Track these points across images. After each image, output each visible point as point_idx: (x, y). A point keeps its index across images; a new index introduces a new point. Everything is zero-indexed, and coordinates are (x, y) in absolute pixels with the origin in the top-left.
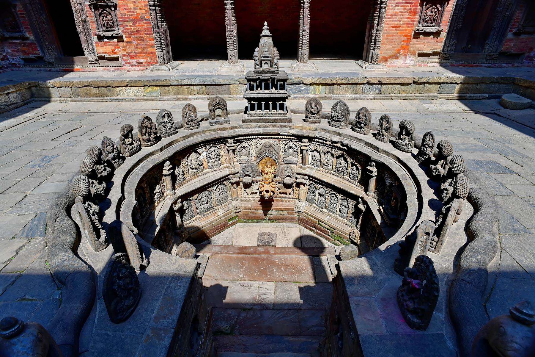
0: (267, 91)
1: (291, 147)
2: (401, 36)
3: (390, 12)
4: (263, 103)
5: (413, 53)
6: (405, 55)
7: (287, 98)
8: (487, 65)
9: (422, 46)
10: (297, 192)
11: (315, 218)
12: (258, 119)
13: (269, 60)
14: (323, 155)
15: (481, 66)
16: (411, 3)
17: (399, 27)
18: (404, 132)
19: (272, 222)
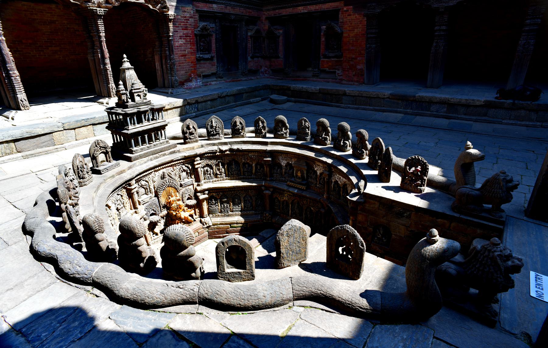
0: (140, 125)
1: (184, 171)
2: (189, 62)
3: (177, 44)
4: (146, 136)
5: (200, 76)
6: (195, 78)
7: (166, 125)
8: (244, 79)
9: (204, 69)
12: (147, 153)
13: (140, 92)
14: (214, 167)
15: (242, 80)
16: (189, 36)
17: (186, 55)
18: (280, 125)
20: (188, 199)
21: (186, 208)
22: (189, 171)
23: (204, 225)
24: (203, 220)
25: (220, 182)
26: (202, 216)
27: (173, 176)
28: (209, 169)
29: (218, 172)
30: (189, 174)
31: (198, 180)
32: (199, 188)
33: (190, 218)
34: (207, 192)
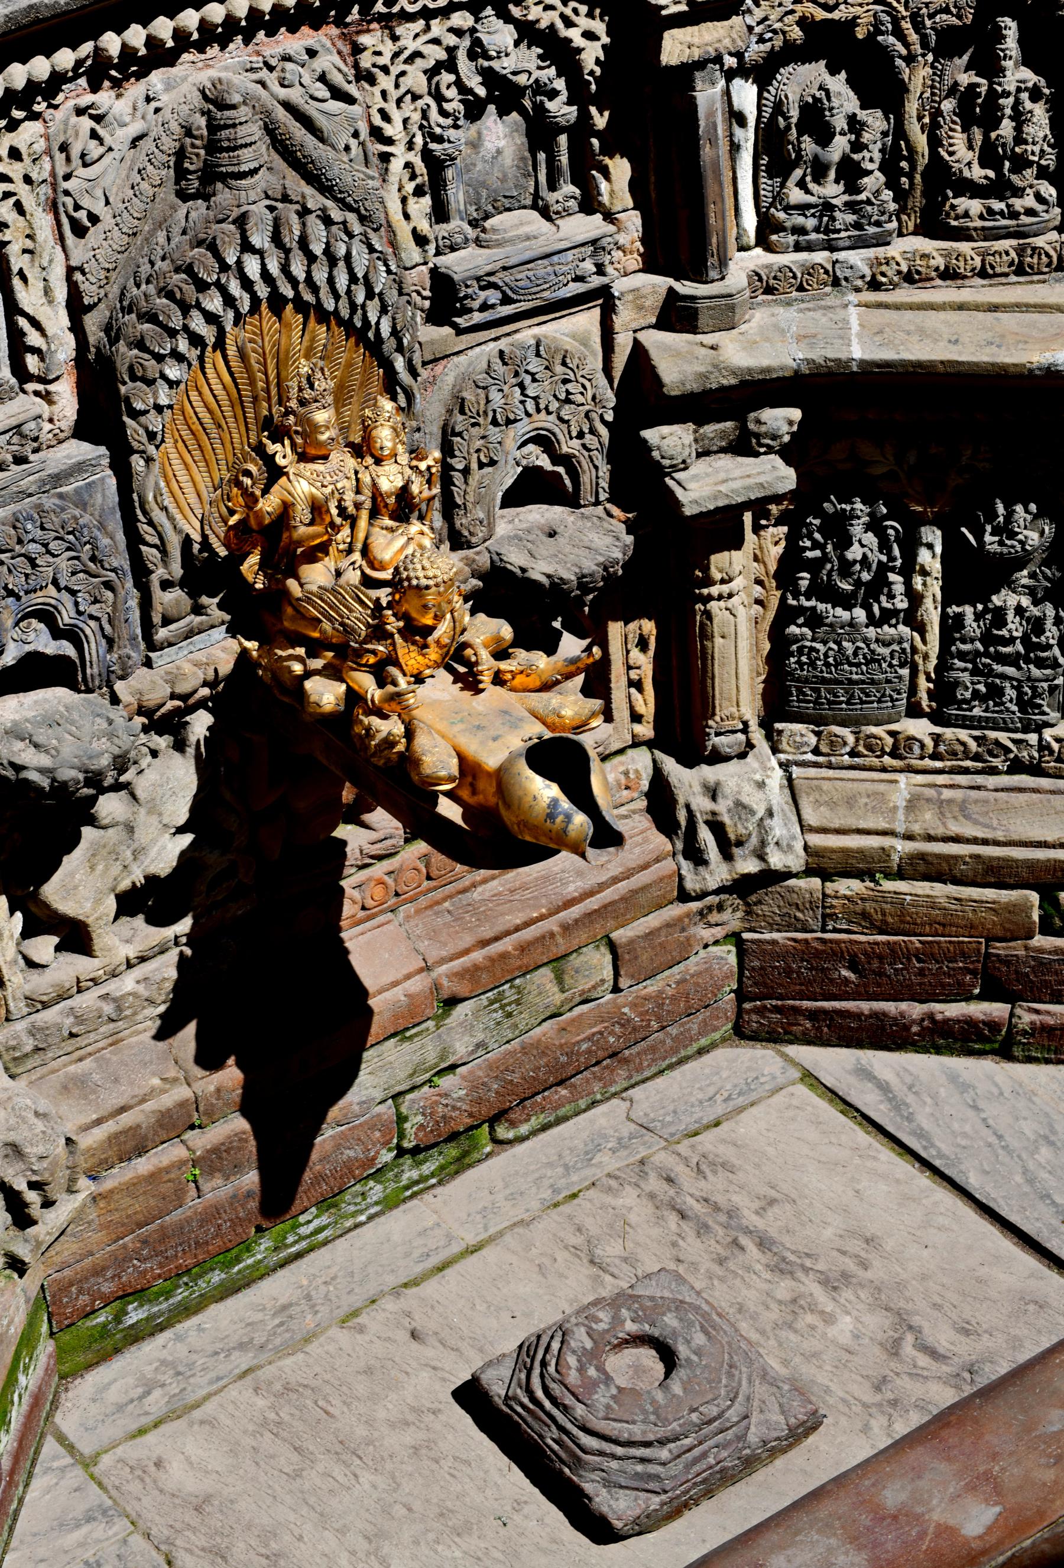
1: (504, 94)
10: (644, 663)
11: (996, 874)
14: (918, 79)
19: (461, 1165)
20: (514, 498)
21: (486, 630)
22: (561, 109)
23: (695, 855)
24: (687, 782)
25: (976, 292)
26: (683, 725)
27: (344, 167)
28: (844, 100)
29: (962, 152)
30: (560, 156)
31: (679, 240)
32: (680, 361)
33: (543, 791)
34: (781, 419)
